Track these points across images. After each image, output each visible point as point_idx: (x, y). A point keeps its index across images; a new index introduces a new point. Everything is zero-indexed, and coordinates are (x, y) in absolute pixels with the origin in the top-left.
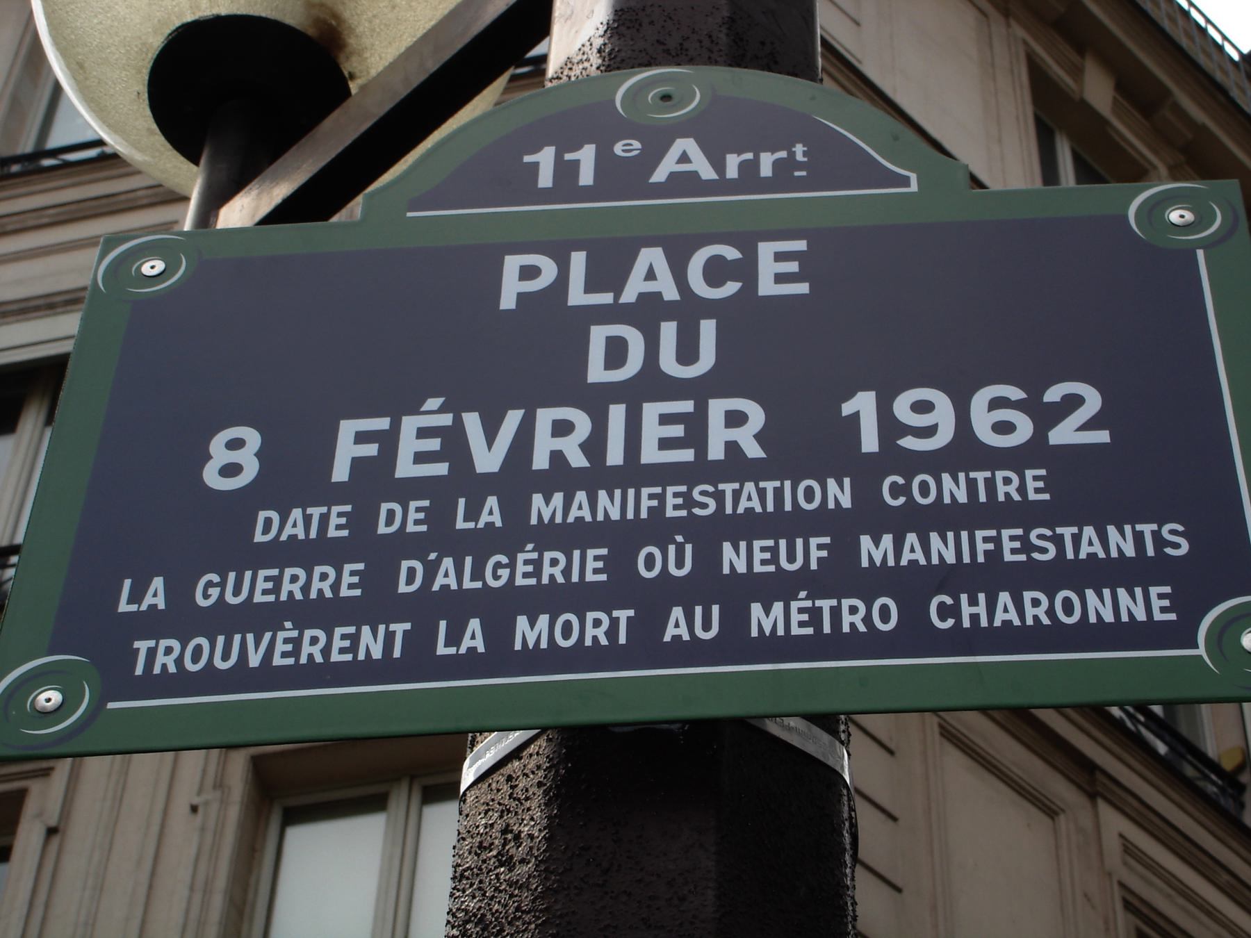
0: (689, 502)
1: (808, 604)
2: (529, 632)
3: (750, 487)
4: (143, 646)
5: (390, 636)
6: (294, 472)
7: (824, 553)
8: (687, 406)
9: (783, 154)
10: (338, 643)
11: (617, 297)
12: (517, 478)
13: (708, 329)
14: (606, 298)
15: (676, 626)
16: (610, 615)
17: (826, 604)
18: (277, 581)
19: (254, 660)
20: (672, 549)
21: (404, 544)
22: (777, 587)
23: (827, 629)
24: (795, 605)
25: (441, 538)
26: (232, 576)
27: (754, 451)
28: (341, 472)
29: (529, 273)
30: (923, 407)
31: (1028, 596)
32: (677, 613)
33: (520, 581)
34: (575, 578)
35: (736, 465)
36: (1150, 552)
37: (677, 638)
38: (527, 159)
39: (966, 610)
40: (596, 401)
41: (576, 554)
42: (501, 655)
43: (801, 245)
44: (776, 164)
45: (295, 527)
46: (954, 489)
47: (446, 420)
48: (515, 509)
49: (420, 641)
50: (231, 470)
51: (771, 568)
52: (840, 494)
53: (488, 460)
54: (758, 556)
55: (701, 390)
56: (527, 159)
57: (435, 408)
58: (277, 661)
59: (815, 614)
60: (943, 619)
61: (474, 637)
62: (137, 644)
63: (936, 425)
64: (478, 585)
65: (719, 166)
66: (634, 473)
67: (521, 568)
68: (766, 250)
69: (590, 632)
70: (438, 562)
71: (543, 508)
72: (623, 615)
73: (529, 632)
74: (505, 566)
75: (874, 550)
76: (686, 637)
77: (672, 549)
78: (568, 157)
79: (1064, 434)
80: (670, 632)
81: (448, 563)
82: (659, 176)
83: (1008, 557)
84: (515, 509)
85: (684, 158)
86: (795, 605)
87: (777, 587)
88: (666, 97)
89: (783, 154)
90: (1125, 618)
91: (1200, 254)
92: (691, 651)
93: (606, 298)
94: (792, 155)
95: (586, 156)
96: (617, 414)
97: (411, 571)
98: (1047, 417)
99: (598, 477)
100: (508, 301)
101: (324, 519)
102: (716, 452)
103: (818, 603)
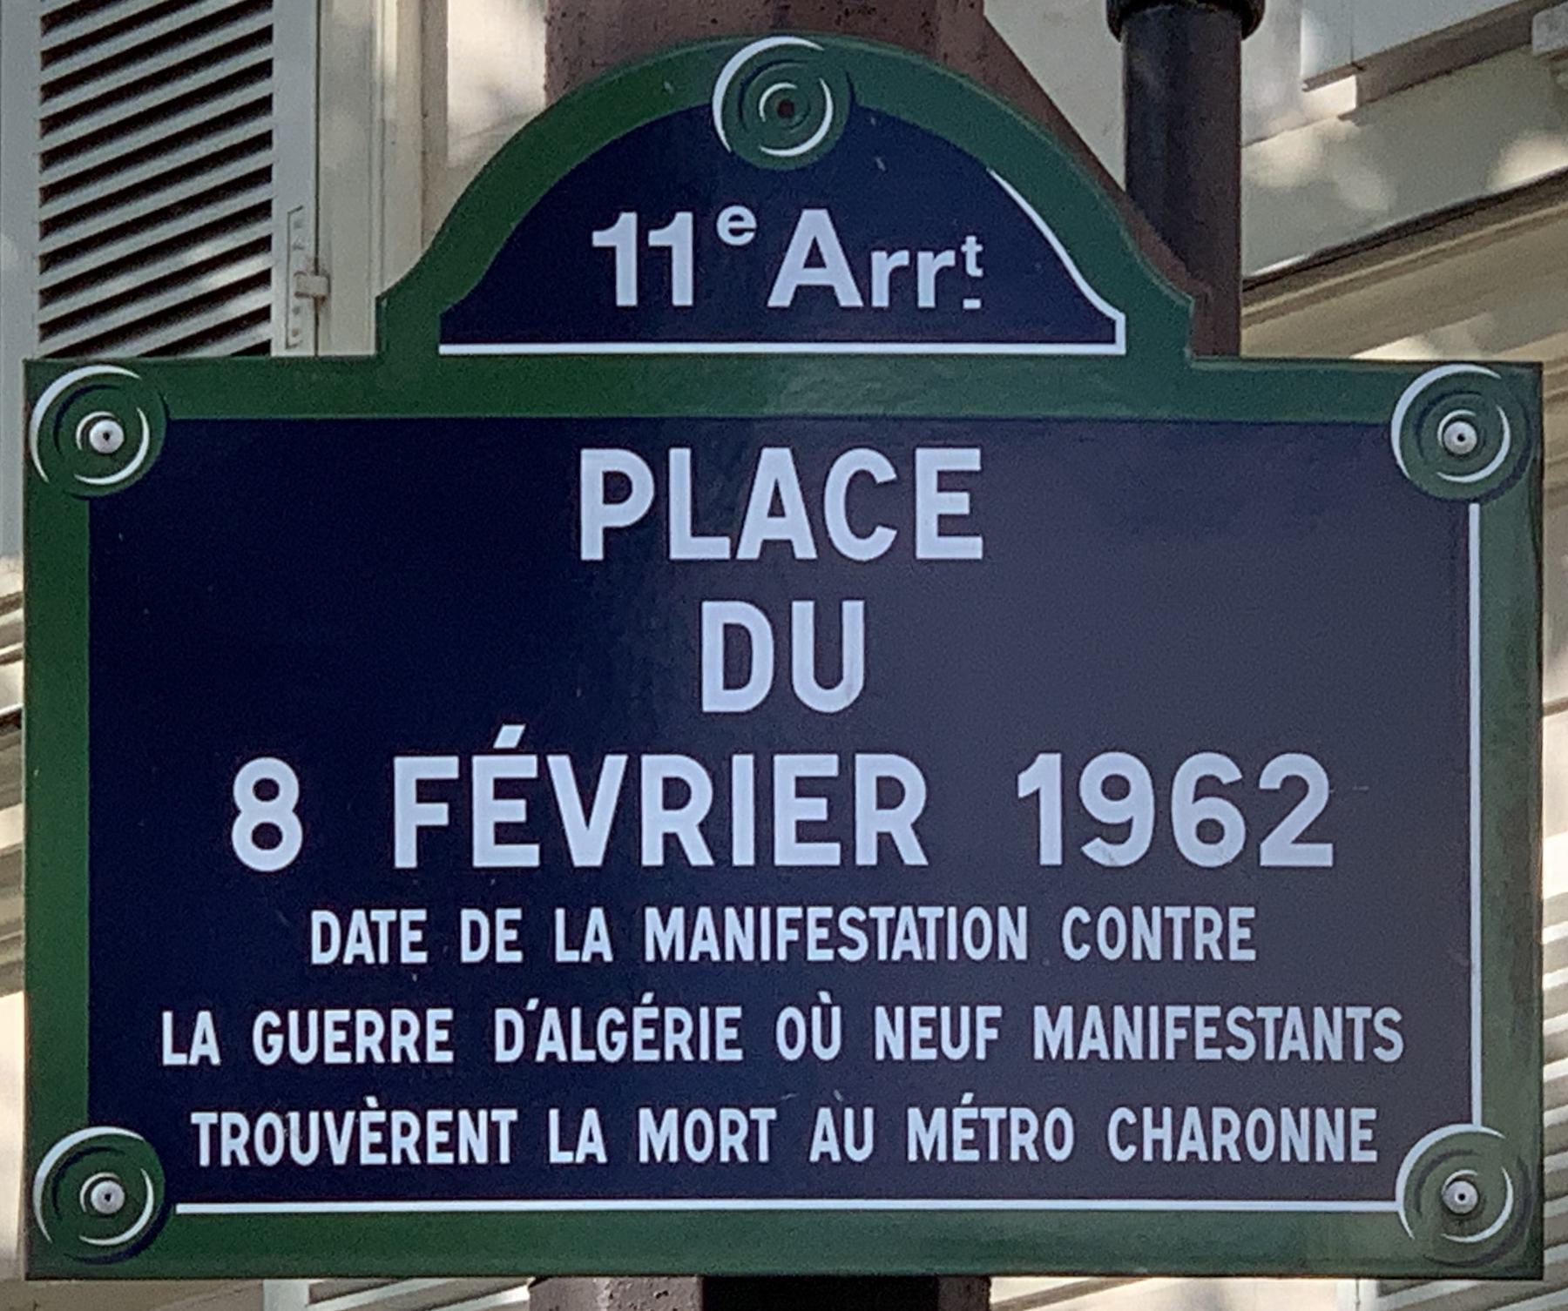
0: (836, 940)
1: (972, 1113)
2: (657, 1135)
3: (907, 911)
4: (202, 1120)
5: (494, 1127)
6: (345, 856)
7: (993, 1034)
8: (826, 765)
9: (948, 258)
10: (436, 1137)
11: (734, 549)
12: (625, 884)
13: (853, 612)
14: (715, 548)
15: (822, 1145)
16: (747, 1115)
17: (993, 1114)
18: (348, 1027)
19: (339, 1157)
20: (816, 1012)
21: (495, 985)
22: (934, 1084)
23: (994, 1155)
26: (293, 1016)
27: (913, 855)
28: (406, 856)
29: (617, 487)
30: (1116, 788)
31: (1219, 1114)
32: (825, 1116)
33: (640, 1055)
34: (704, 1056)
35: (887, 881)
36: (1359, 1055)
37: (825, 1156)
38: (600, 239)
39: (1150, 1134)
40: (715, 742)
41: (704, 1012)
42: (622, 1171)
43: (969, 459)
44: (942, 274)
45: (359, 948)
46: (1146, 936)
47: (525, 767)
48: (626, 933)
49: (529, 1136)
50: (267, 836)
51: (931, 1054)
52: (1013, 935)
53: (587, 844)
56: (600, 239)
57: (513, 744)
58: (367, 1158)
59: (980, 1126)
60: (1123, 1147)
61: (592, 1144)
62: (196, 1118)
63: (1129, 823)
64: (590, 1056)
66: (767, 885)
69: (727, 1141)
70: (539, 1014)
71: (662, 933)
73: (657, 1135)
74: (620, 1028)
75: (1051, 1032)
76: (836, 1157)
77: (816, 1012)
78: (656, 238)
79: (1280, 849)
80: (817, 1149)
81: (551, 1015)
82: (781, 296)
83: (1202, 1053)
84: (626, 933)
85: (815, 259)
86: (959, 1114)
87: (934, 1084)
89: (948, 258)
91: (1474, 509)
92: (839, 1177)
93: (715, 548)
94: (961, 258)
95: (678, 234)
96: (743, 767)
97: (509, 1026)
98: (1264, 810)
99: (723, 887)
100: (592, 549)
101: (394, 927)
102: (866, 855)
103: (986, 1113)
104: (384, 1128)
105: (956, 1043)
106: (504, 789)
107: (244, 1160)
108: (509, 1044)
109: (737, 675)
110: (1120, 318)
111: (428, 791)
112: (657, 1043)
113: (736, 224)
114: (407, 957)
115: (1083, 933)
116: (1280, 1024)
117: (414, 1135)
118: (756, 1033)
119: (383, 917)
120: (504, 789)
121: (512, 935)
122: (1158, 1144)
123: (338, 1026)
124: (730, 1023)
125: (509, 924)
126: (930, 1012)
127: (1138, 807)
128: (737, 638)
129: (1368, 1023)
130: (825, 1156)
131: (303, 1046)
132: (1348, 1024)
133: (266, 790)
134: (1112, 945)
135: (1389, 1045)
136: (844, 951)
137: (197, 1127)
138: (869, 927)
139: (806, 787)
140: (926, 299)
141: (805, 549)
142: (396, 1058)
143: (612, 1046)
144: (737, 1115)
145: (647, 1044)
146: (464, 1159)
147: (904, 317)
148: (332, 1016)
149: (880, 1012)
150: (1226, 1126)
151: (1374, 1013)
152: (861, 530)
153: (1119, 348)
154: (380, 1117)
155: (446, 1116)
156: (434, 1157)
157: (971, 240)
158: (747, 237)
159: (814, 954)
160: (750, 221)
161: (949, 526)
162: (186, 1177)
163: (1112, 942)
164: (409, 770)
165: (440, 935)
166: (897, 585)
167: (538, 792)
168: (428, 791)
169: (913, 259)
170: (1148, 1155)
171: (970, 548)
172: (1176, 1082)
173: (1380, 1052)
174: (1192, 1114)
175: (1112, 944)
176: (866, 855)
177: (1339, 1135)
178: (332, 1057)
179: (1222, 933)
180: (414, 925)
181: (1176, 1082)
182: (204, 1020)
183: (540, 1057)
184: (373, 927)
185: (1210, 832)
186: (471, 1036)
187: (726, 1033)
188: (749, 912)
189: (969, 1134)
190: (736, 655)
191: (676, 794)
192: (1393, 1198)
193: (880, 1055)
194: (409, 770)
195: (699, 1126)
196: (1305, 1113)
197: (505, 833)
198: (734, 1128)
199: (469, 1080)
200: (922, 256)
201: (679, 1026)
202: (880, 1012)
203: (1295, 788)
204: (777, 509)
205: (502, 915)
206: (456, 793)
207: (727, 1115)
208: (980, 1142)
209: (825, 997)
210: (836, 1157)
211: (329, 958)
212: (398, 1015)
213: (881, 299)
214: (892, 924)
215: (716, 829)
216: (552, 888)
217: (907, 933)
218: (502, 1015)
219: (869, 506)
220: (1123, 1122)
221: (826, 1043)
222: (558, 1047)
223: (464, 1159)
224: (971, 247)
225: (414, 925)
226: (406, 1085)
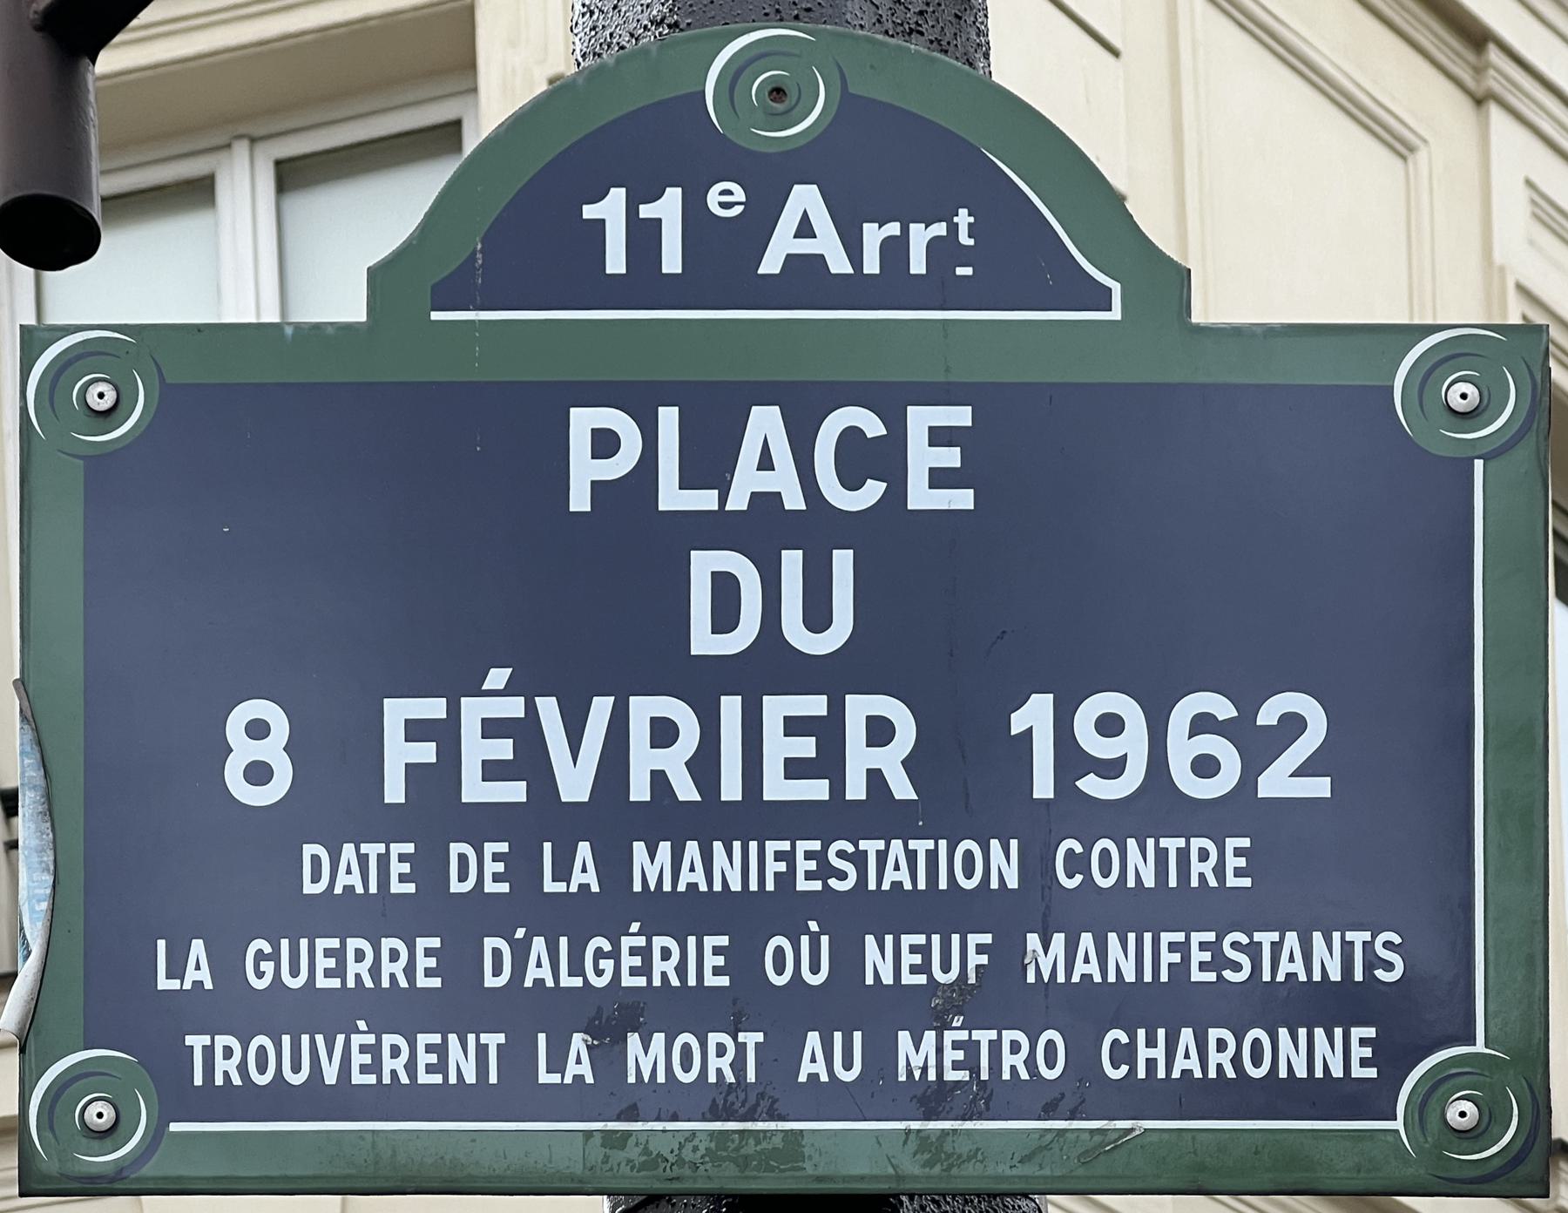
0: (825, 871)
1: (963, 1035)
3: (897, 845)
5: (482, 1050)
7: (984, 960)
8: (815, 705)
9: (940, 229)
10: (424, 1059)
11: (723, 500)
12: (614, 818)
13: (843, 562)
14: (706, 500)
15: (811, 1066)
16: (735, 1039)
17: (984, 1036)
18: (339, 954)
19: (331, 1076)
20: (805, 939)
21: (481, 914)
22: (929, 1009)
24: (949, 1037)
25: (526, 910)
26: (285, 943)
27: (902, 788)
28: (395, 791)
29: (605, 444)
30: (1110, 725)
32: (813, 1039)
33: (627, 981)
34: (692, 982)
35: (880, 814)
37: (813, 1077)
38: (589, 212)
39: (1143, 1053)
40: (702, 684)
41: (692, 940)
43: (961, 416)
44: (933, 245)
46: (1140, 866)
47: (514, 707)
48: (614, 865)
49: (517, 1058)
50: (259, 773)
51: (922, 979)
52: (1004, 866)
53: (575, 781)
54: (909, 959)
56: (589, 212)
58: (357, 1078)
59: (971, 1047)
60: (1116, 1066)
64: (577, 982)
65: (854, 250)
66: (756, 819)
67: (628, 961)
68: (920, 419)
69: (714, 1063)
70: (526, 944)
71: (649, 865)
74: (607, 956)
76: (824, 1078)
77: (805, 939)
78: (646, 211)
81: (539, 944)
82: (771, 264)
84: (614, 865)
85: (805, 229)
86: (949, 1037)
87: (929, 1009)
88: (778, 92)
89: (940, 229)
92: (829, 1099)
93: (706, 500)
94: (953, 229)
95: (668, 208)
96: (731, 708)
97: (497, 953)
98: (1259, 748)
99: (710, 821)
100: (580, 501)
101: (384, 860)
102: (856, 790)
103: (976, 1035)
104: (374, 1050)
105: (946, 968)
106: (492, 728)
108: (497, 972)
109: (725, 619)
111: (416, 730)
112: (645, 970)
113: (726, 198)
114: (396, 887)
115: (1076, 864)
117: (401, 1057)
118: (742, 961)
119: (373, 850)
120: (492, 728)
121: (500, 867)
122: (1151, 1063)
123: (328, 953)
125: (496, 857)
126: (920, 939)
127: (1133, 743)
128: (725, 587)
130: (813, 1077)
131: (295, 972)
134: (1106, 875)
136: (833, 882)
138: (859, 859)
139: (794, 726)
140: (918, 266)
141: (794, 501)
142: (386, 983)
143: (599, 973)
144: (726, 1039)
145: (634, 972)
146: (453, 1080)
147: (893, 284)
149: (870, 940)
150: (1221, 1045)
151: (1374, 937)
152: (851, 481)
154: (370, 1039)
155: (436, 1039)
156: (424, 1078)
157: (963, 212)
158: (738, 210)
159: (802, 885)
160: (739, 194)
161: (939, 478)
162: (180, 1095)
164: (397, 711)
166: (888, 537)
167: (527, 732)
168: (416, 730)
169: (905, 230)
170: (1141, 1074)
171: (964, 499)
172: (1167, 1004)
174: (1187, 1035)
176: (856, 790)
178: (322, 982)
179: (1220, 862)
180: (402, 858)
183: (528, 983)
184: (363, 860)
185: (1205, 766)
186: (459, 963)
187: (712, 961)
188: (737, 845)
190: (723, 602)
193: (869, 980)
194: (397, 711)
195: (686, 1049)
197: (493, 771)
199: (458, 1005)
201: (666, 954)
202: (870, 940)
204: (766, 463)
205: (490, 848)
206: (445, 734)
207: (714, 1038)
209: (813, 926)
210: (824, 1078)
211: (320, 887)
212: (387, 944)
213: (872, 265)
214: (882, 857)
215: (705, 765)
216: (541, 822)
217: (897, 865)
218: (490, 943)
219: (858, 458)
220: (1116, 1042)
221: (815, 969)
222: (546, 973)
223: (453, 1080)
224: (963, 218)
225: (402, 858)
226: (396, 1010)
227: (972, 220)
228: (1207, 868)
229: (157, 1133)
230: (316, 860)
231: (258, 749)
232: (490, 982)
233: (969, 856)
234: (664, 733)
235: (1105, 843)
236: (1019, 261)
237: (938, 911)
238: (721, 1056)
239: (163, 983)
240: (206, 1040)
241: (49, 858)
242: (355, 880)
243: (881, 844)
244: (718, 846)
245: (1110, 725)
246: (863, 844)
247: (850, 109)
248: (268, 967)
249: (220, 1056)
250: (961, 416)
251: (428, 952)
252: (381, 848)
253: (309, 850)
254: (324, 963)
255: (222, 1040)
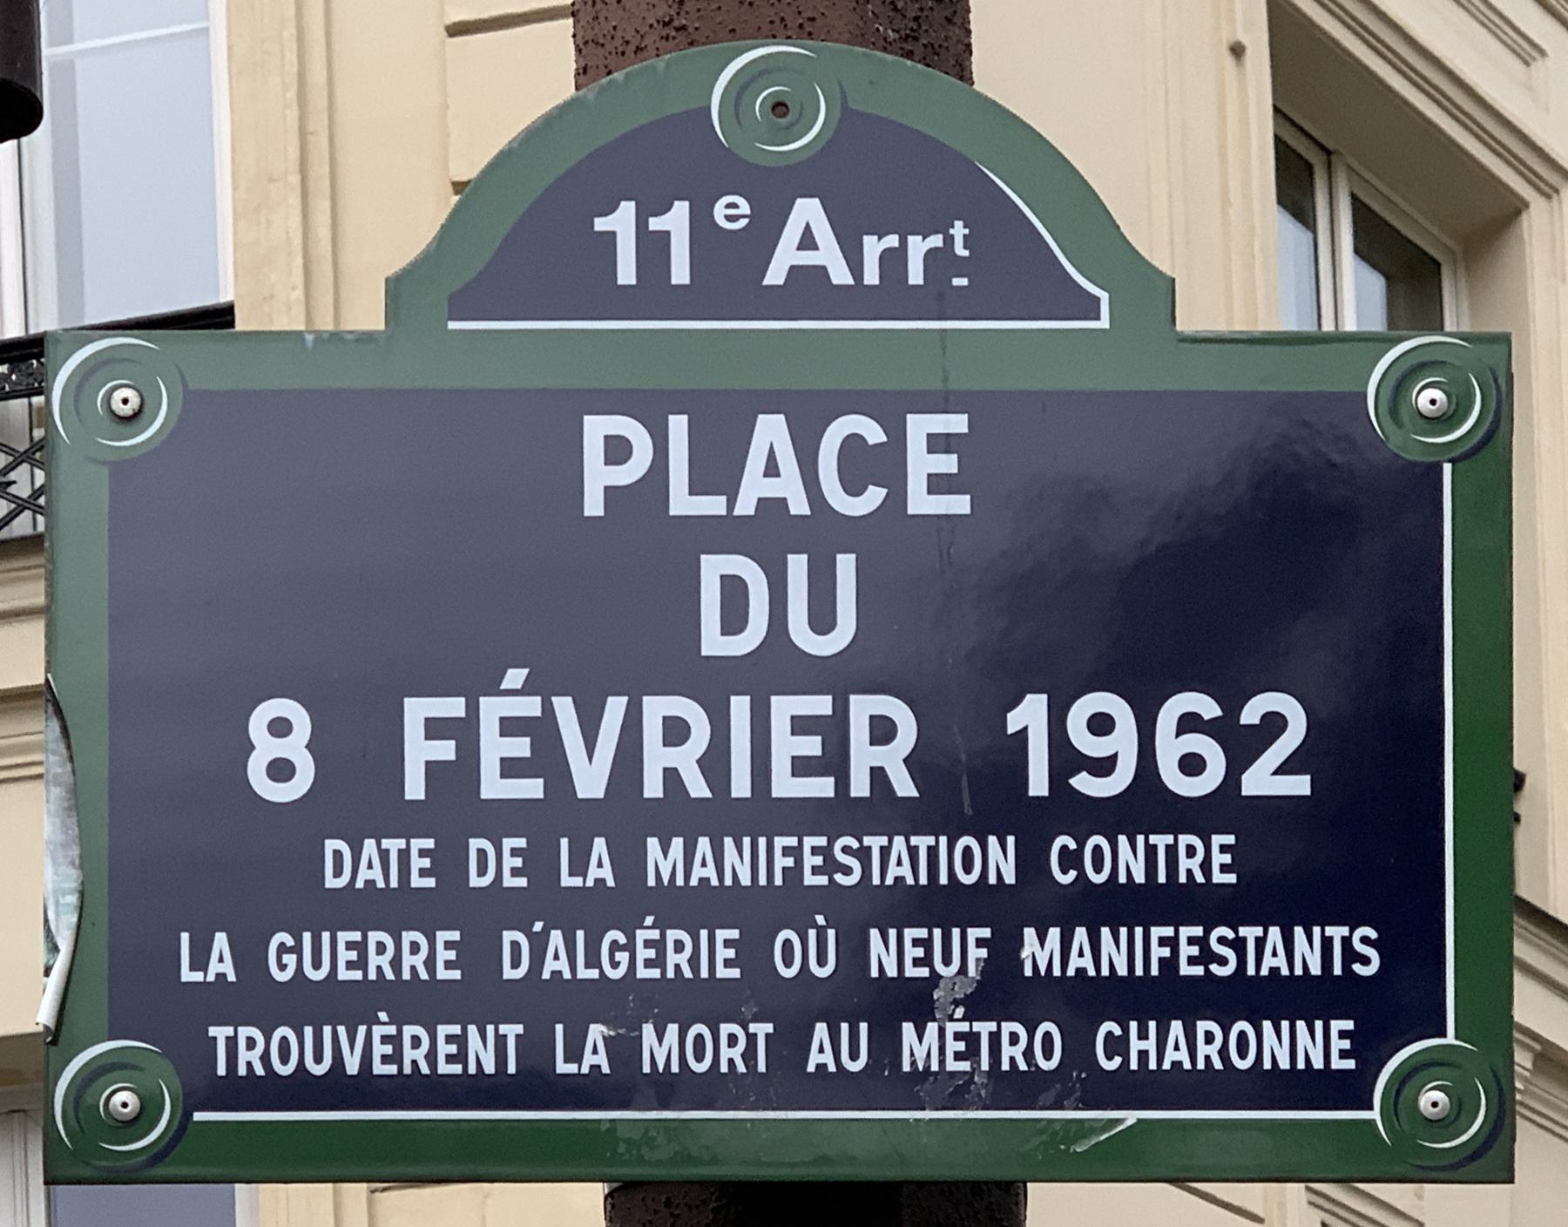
0: (830, 866)
1: (964, 1027)
4: (220, 1033)
5: (501, 1040)
7: (983, 953)
8: (821, 705)
9: (936, 241)
10: (444, 1049)
11: (731, 505)
12: (629, 814)
13: (846, 565)
14: (714, 505)
15: (819, 1057)
16: (745, 1028)
17: (984, 1028)
18: (361, 947)
19: (352, 1066)
20: (812, 933)
21: (501, 908)
25: (544, 904)
26: (307, 936)
27: (905, 787)
28: (415, 788)
29: (617, 450)
32: (821, 1030)
33: (642, 973)
34: (704, 974)
35: (883, 811)
36: (1337, 971)
38: (601, 224)
39: (1135, 1045)
40: (712, 684)
41: (704, 933)
43: (957, 423)
44: (931, 255)
47: (530, 707)
48: (629, 860)
50: (281, 770)
51: (924, 972)
54: (912, 952)
55: (840, 678)
56: (601, 224)
58: (379, 1068)
59: (971, 1039)
62: (213, 1031)
64: (594, 974)
65: (855, 262)
66: (766, 815)
67: (643, 954)
68: (919, 426)
69: (726, 1053)
70: (545, 933)
71: (663, 861)
72: (762, 1029)
73: (659, 1048)
74: (622, 948)
75: (1039, 951)
76: (832, 1068)
77: (812, 933)
78: (655, 224)
79: (1261, 780)
81: (556, 937)
82: (775, 275)
83: (1185, 970)
84: (629, 860)
85: (808, 241)
88: (779, 107)
89: (936, 241)
90: (1301, 1065)
92: (835, 1088)
93: (714, 505)
94: (949, 240)
95: (676, 221)
96: (740, 706)
97: (515, 946)
98: (1243, 746)
99: (721, 818)
100: (594, 505)
101: (404, 855)
102: (860, 787)
103: (977, 1026)
104: (395, 1040)
106: (510, 727)
107: (260, 1071)
108: (515, 964)
109: (734, 621)
110: (1104, 296)
111: (435, 729)
112: (659, 962)
114: (417, 882)
115: (1070, 859)
116: (1260, 943)
117: (422, 1048)
118: (752, 953)
119: (394, 845)
120: (510, 727)
121: (518, 862)
122: (1143, 1055)
123: (350, 946)
124: (728, 943)
125: (515, 852)
126: (922, 933)
127: (1123, 742)
128: (734, 589)
129: (1347, 942)
130: (821, 1067)
131: (317, 965)
132: (1327, 943)
133: (280, 728)
135: (1366, 961)
137: (215, 1038)
139: (801, 725)
140: (916, 276)
141: (799, 506)
142: (406, 975)
144: (735, 1028)
147: (892, 296)
148: (344, 937)
149: (874, 933)
150: (1209, 1038)
152: (853, 488)
153: (1104, 323)
155: (456, 1029)
156: (444, 1068)
157: (959, 224)
158: (743, 223)
159: (810, 880)
160: (744, 208)
161: (938, 484)
163: (1098, 868)
164: (417, 710)
165: (448, 862)
166: (888, 541)
167: (543, 730)
168: (435, 729)
170: (1134, 1066)
171: (960, 504)
172: (1161, 997)
173: (1357, 968)
174: (1176, 1027)
175: (1098, 868)
176: (860, 787)
177: (1319, 1045)
178: (344, 974)
180: (423, 853)
181: (1161, 997)
182: (221, 940)
183: (546, 975)
184: (384, 855)
185: (1192, 765)
186: (478, 955)
187: (724, 953)
189: (961, 1046)
191: (676, 732)
192: (1371, 1108)
194: (417, 710)
196: (1285, 1024)
197: (510, 768)
198: (733, 1041)
199: (477, 996)
200: (911, 238)
202: (874, 933)
203: (1274, 724)
204: (772, 470)
205: (509, 843)
206: (464, 732)
207: (726, 1029)
208: (971, 1053)
209: (820, 920)
210: (832, 1068)
211: (341, 882)
212: (408, 937)
213: (872, 277)
214: (885, 852)
216: (557, 818)
217: (901, 860)
218: (508, 936)
219: (860, 465)
220: (1109, 1034)
221: (822, 962)
222: (563, 965)
223: (472, 1070)
224: (959, 230)
225: (423, 853)
226: (415, 1001)
227: (967, 231)
228: (1194, 864)
229: (182, 1124)
230: (338, 855)
231: (280, 747)
232: (509, 973)
233: (967, 851)
234: (676, 732)
235: (1098, 839)
236: (1011, 272)
237: (940, 905)
238: (733, 1046)
239: (188, 975)
240: (229, 1031)
241: (75, 852)
242: (376, 874)
243: (884, 840)
244: (728, 842)
245: (1101, 725)
246: (867, 841)
247: (851, 124)
248: (291, 960)
249: (245, 1048)
250: (957, 423)
251: (449, 945)
252: (402, 843)
253: (331, 845)
254: (345, 955)
255: (245, 1032)
